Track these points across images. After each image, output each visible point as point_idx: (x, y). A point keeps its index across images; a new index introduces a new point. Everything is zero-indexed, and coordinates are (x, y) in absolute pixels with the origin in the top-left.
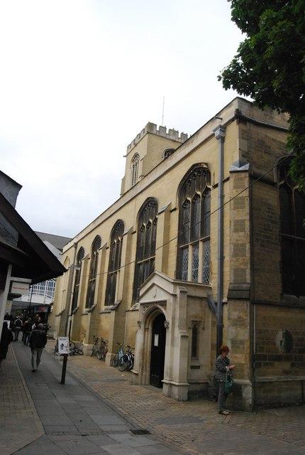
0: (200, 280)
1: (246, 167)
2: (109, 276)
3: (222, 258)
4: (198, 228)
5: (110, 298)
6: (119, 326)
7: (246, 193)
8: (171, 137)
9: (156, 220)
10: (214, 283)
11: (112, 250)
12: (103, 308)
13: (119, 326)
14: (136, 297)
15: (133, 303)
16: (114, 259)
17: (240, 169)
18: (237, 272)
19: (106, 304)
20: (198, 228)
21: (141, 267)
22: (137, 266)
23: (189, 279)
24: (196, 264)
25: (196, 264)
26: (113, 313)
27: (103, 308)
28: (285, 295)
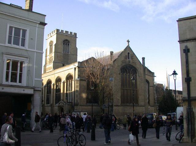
0: (71, 101)
1: (79, 79)
2: (47, 96)
3: (74, 97)
4: (70, 89)
5: (48, 102)
6: (52, 110)
7: (79, 85)
8: (66, 34)
9: (60, 83)
10: (73, 101)
11: (47, 87)
12: (46, 105)
13: (52, 110)
14: (56, 103)
15: (55, 104)
16: (48, 90)
17: (77, 79)
18: (77, 100)
19: (47, 104)
20: (70, 89)
21: (57, 95)
22: (56, 94)
23: (69, 101)
24: (70, 97)
25: (70, 97)
26: (50, 107)
27: (46, 105)
28: (87, 104)
